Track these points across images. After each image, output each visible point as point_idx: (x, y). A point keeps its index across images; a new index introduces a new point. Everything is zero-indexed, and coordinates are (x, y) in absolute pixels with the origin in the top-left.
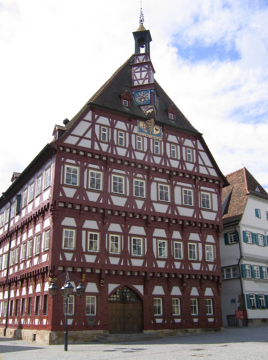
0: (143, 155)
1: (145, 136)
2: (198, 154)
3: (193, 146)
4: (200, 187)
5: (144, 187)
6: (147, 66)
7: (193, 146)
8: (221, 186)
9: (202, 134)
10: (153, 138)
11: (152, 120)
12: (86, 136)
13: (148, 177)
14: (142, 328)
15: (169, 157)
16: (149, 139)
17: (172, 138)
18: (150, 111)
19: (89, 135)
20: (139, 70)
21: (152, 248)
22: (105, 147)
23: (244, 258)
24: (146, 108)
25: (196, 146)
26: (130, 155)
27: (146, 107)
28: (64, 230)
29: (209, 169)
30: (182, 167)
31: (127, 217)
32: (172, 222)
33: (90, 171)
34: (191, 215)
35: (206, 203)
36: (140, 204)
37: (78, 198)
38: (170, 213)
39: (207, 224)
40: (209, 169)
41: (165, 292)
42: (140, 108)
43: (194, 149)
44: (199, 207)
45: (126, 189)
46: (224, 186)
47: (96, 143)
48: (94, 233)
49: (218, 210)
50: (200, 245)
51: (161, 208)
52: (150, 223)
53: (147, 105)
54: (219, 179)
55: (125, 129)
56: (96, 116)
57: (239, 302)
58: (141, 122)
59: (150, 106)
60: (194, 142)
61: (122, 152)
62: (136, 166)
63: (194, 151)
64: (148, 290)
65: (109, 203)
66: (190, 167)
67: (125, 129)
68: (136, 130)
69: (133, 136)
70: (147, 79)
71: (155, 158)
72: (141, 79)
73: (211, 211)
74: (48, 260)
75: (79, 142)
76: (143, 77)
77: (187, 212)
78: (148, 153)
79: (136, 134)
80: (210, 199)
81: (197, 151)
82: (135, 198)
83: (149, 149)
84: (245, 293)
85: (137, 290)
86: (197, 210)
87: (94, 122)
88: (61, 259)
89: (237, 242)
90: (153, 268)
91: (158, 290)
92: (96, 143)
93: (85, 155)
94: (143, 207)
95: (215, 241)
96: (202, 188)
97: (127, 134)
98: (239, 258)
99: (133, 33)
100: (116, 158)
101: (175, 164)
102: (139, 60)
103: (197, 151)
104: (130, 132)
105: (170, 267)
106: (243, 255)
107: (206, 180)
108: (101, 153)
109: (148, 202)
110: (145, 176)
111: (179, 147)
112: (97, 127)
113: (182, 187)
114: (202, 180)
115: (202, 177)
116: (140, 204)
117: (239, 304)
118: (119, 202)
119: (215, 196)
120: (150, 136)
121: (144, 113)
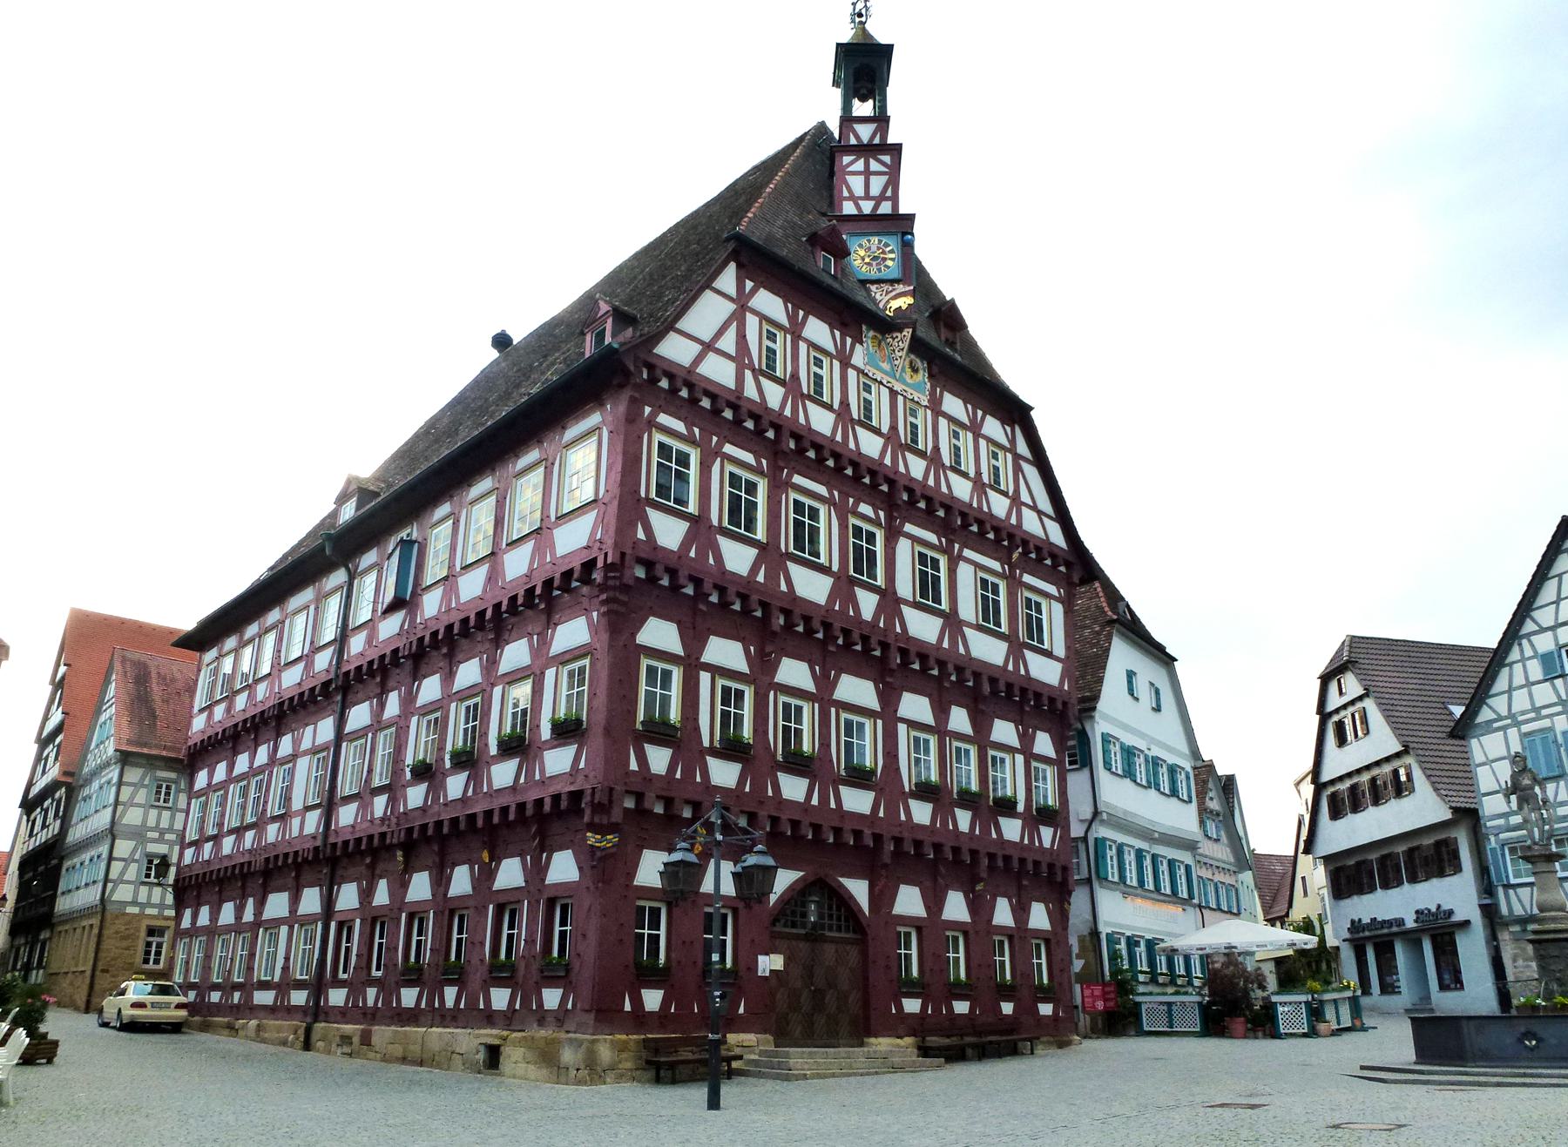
0: (880, 441)
3: (1007, 445)
5: (879, 548)
6: (887, 159)
7: (1007, 445)
8: (1076, 579)
11: (908, 333)
12: (720, 345)
13: (890, 518)
14: (861, 1028)
17: (953, 405)
18: (904, 302)
19: (728, 343)
20: (859, 165)
21: (896, 756)
22: (774, 395)
23: (1105, 816)
25: (1013, 441)
27: (886, 287)
28: (645, 662)
29: (1045, 520)
31: (835, 641)
32: (949, 678)
33: (729, 468)
34: (998, 660)
35: (1035, 627)
36: (868, 603)
37: (692, 554)
38: (946, 645)
39: (1038, 696)
41: (927, 908)
42: (868, 291)
43: (1010, 451)
45: (829, 546)
46: (1083, 582)
47: (748, 373)
48: (734, 685)
49: (1067, 657)
50: (1020, 758)
51: (923, 627)
52: (892, 671)
53: (892, 282)
54: (1071, 559)
56: (749, 284)
57: (1078, 957)
58: (871, 333)
59: (901, 288)
61: (821, 421)
62: (857, 478)
63: (1009, 456)
64: (882, 898)
65: (784, 587)
66: (999, 506)
68: (858, 358)
69: (852, 374)
70: (887, 199)
72: (867, 197)
73: (1048, 654)
74: (582, 765)
75: (699, 359)
76: (875, 190)
77: (988, 650)
79: (860, 371)
80: (1044, 617)
81: (1017, 458)
82: (853, 582)
83: (894, 427)
84: (1104, 930)
85: (851, 897)
86: (1016, 649)
87: (742, 305)
88: (634, 766)
89: (1083, 766)
90: (901, 824)
92: (748, 373)
93: (716, 412)
96: (1027, 578)
97: (836, 364)
98: (1088, 816)
99: (838, 45)
100: (805, 438)
101: (962, 489)
102: (857, 137)
103: (1017, 458)
105: (945, 823)
106: (1101, 807)
107: (1033, 554)
108: (760, 414)
109: (889, 600)
110: (882, 514)
111: (970, 435)
112: (752, 322)
113: (977, 566)
114: (1025, 553)
115: (1026, 541)
116: (868, 603)
117: (1082, 962)
118: (812, 587)
119: (1058, 609)
120: (898, 387)
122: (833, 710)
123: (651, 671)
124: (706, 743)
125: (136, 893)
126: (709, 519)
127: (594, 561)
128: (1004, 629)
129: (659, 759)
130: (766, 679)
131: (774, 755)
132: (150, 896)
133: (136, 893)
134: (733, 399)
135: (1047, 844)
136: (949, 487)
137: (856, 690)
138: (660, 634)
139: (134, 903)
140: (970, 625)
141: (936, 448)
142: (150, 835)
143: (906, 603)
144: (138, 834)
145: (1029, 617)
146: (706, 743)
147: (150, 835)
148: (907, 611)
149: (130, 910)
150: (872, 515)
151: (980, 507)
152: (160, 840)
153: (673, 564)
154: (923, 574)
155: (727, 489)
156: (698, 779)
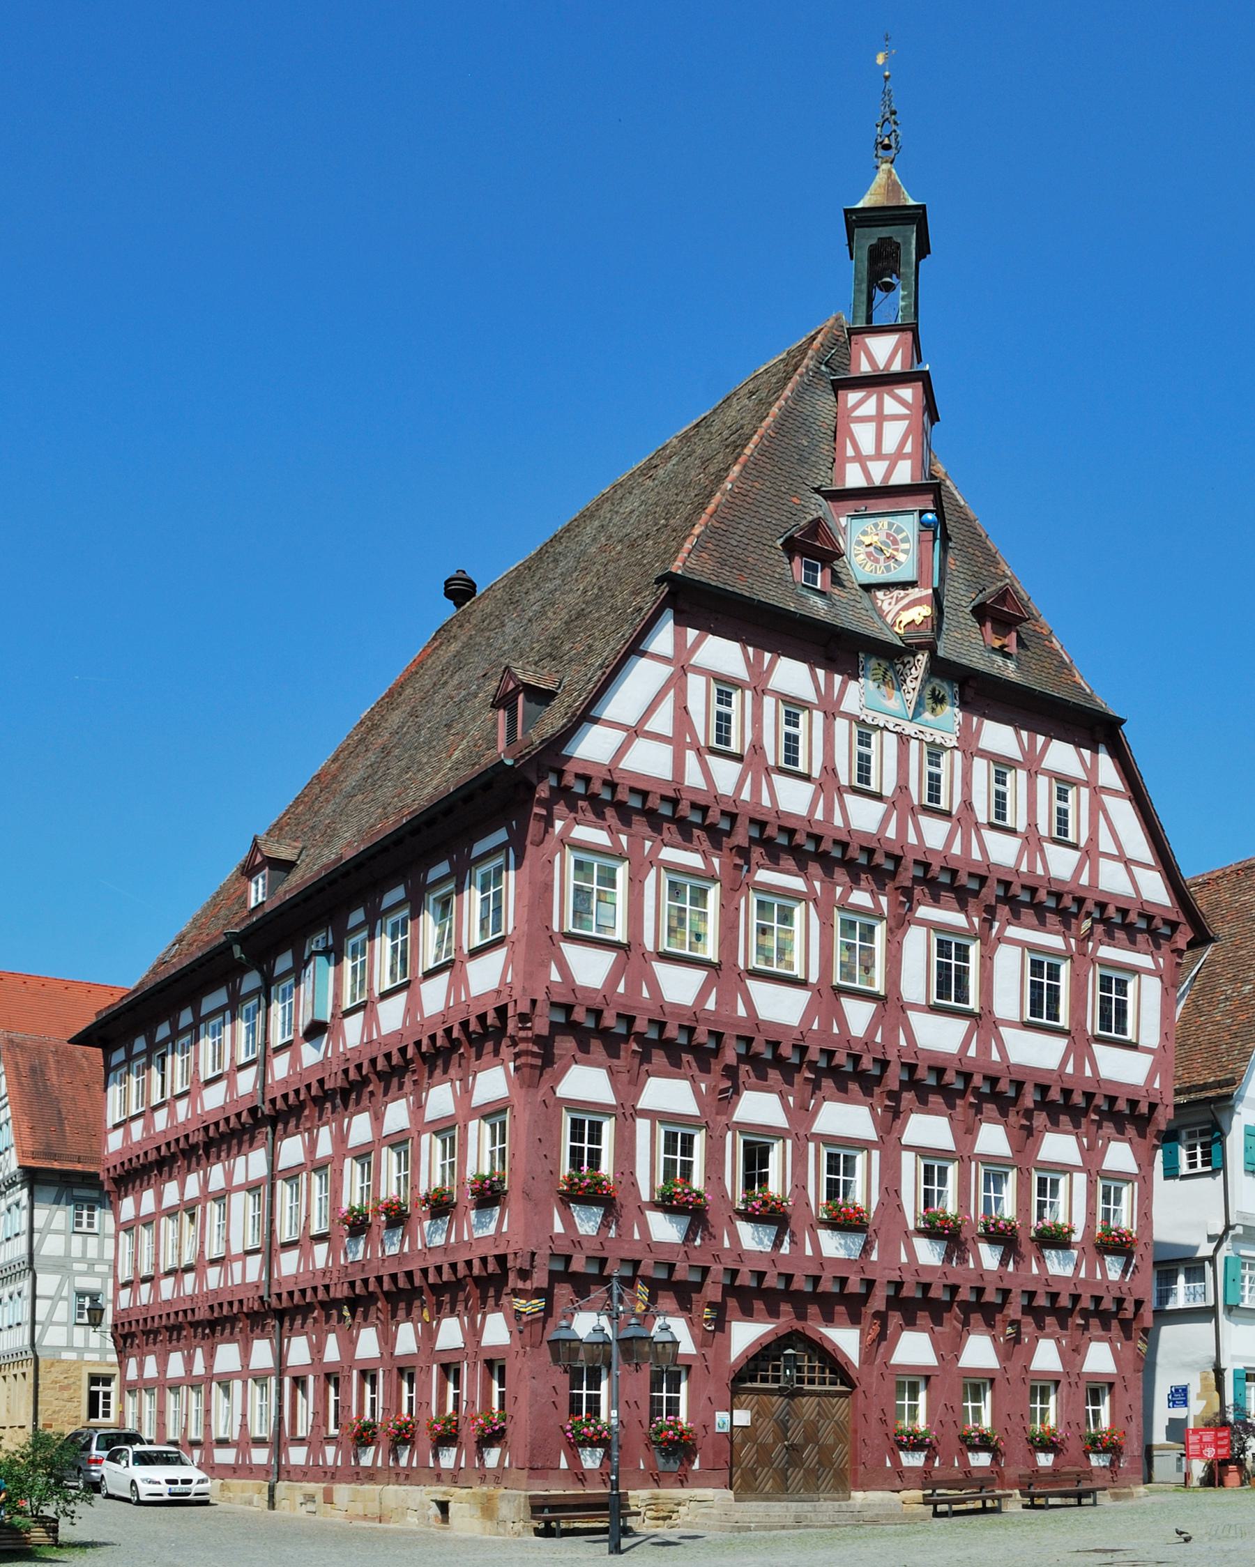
1: (891, 727)
2: (1097, 808)
4: (1095, 949)
9: (1122, 721)
10: (921, 736)
11: (923, 658)
15: (982, 818)
16: (903, 739)
24: (898, 601)
25: (1092, 771)
26: (829, 811)
30: (1031, 862)
35: (1114, 1015)
36: (858, 1016)
37: (621, 989)
38: (972, 1052)
42: (873, 601)
43: (1086, 784)
44: (1086, 1030)
51: (940, 1036)
53: (904, 585)
58: (873, 663)
59: (915, 593)
60: (1086, 753)
63: (1085, 792)
65: (742, 1011)
66: (1061, 864)
74: (505, 1229)
77: (1037, 1052)
78: (899, 802)
82: (841, 991)
83: (902, 788)
94: (871, 1030)
95: (1139, 1165)
103: (1098, 792)
116: (858, 1016)
118: (781, 1007)
120: (910, 729)
121: (889, 619)
122: (811, 1146)
123: (577, 1125)
124: (645, 1197)
125: (70, 1336)
126: (641, 945)
127: (506, 1005)
128: (1064, 1021)
129: (587, 1222)
130: (723, 1119)
131: (733, 1203)
132: (87, 1339)
133: (70, 1336)
134: (671, 794)
136: (983, 850)
137: (846, 1118)
138: (586, 1082)
139: (70, 1348)
140: (1010, 1024)
141: (967, 805)
142: (77, 1267)
143: (915, 1007)
144: (62, 1266)
145: (1105, 1001)
146: (645, 1197)
147: (77, 1267)
148: (913, 1016)
149: (66, 1355)
150: (870, 904)
151: (1032, 871)
152: (90, 1273)
153: (597, 1003)
154: (943, 968)
155: (666, 902)
156: (637, 1236)
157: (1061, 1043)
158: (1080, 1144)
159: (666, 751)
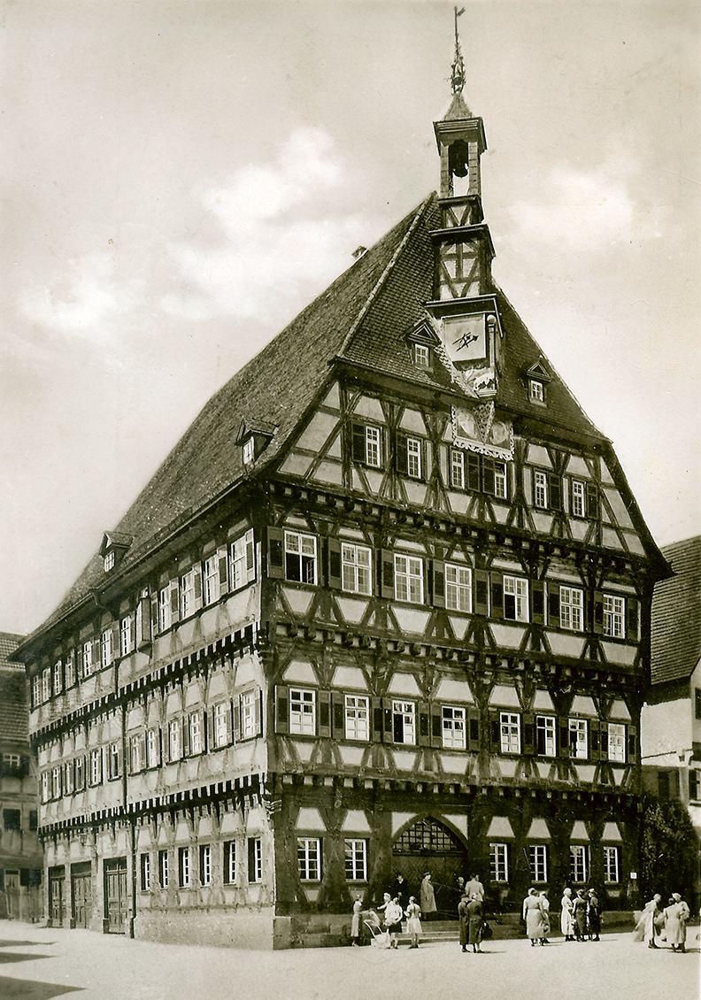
40: (626, 536)
55: (423, 431)
67: (423, 431)
69: (443, 451)
71: (495, 507)
79: (449, 444)
91: (500, 827)
104: (435, 437)
115: (609, 555)
135: (618, 782)
136: (531, 524)
157: (581, 642)
158: (595, 703)
159: (339, 469)
